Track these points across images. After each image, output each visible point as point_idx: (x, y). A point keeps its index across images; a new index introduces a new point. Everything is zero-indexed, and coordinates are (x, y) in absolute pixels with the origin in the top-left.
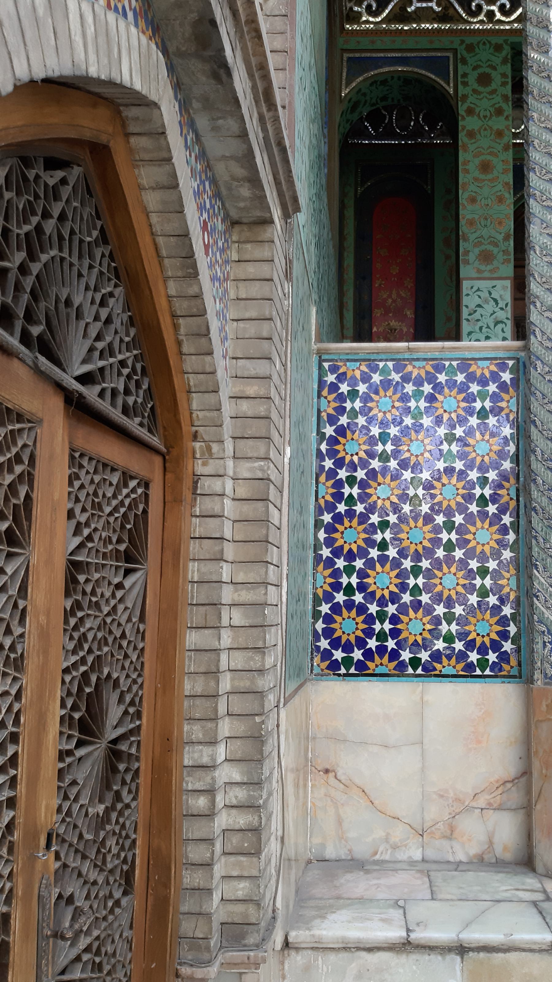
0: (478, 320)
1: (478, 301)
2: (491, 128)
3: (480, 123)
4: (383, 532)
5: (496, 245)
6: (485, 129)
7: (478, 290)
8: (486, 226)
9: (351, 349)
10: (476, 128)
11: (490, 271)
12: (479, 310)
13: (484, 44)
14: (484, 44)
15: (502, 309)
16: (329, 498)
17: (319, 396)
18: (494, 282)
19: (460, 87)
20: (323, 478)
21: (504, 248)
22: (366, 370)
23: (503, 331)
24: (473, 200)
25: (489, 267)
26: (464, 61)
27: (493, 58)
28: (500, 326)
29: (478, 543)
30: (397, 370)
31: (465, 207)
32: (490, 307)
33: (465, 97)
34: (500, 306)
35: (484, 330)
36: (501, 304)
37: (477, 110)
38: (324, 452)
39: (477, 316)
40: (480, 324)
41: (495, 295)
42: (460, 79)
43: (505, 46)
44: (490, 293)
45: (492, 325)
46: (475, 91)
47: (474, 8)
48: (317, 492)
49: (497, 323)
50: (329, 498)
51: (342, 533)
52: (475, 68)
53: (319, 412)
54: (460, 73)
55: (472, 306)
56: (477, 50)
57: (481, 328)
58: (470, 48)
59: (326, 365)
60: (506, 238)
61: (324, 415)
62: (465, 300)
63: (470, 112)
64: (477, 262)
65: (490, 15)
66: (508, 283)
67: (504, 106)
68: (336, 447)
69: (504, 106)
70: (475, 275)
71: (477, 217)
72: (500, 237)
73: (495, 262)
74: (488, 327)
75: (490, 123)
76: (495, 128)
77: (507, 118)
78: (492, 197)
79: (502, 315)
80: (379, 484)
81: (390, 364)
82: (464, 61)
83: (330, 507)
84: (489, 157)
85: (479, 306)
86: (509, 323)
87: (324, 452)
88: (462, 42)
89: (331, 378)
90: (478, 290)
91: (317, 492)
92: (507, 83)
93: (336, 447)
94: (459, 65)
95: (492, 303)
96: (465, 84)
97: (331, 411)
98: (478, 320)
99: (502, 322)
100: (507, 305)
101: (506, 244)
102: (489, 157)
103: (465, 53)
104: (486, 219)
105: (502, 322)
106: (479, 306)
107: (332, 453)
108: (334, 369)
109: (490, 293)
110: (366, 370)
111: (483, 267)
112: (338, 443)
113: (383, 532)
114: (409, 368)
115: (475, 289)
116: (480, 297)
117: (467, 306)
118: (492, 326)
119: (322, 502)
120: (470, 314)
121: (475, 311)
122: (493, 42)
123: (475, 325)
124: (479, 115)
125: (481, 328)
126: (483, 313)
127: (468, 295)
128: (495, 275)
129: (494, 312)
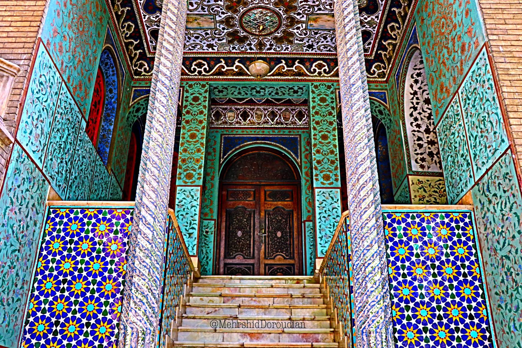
0: (183, 205)
1: (184, 196)
2: (197, 119)
3: (192, 117)
4: (64, 284)
5: (195, 171)
6: (194, 120)
7: (184, 191)
8: (191, 162)
9: (62, 203)
10: (190, 119)
11: (191, 183)
12: (184, 201)
13: (197, 84)
14: (197, 84)
15: (195, 200)
16: (42, 268)
17: (46, 223)
18: (192, 188)
19: (184, 102)
20: (41, 259)
21: (198, 172)
22: (68, 212)
23: (195, 211)
24: (185, 150)
25: (191, 181)
26: (187, 91)
27: (200, 90)
28: (194, 208)
29: (106, 290)
30: (81, 212)
31: (181, 154)
32: (189, 199)
33: (186, 106)
34: (194, 199)
35: (186, 210)
36: (195, 198)
37: (191, 112)
38: (44, 247)
39: (182, 203)
40: (184, 207)
41: (192, 194)
42: (184, 99)
43: (207, 85)
44: (190, 193)
45: (189, 208)
46: (191, 104)
47: (192, 69)
48: (37, 265)
49: (192, 207)
50: (42, 268)
51: (45, 284)
52: (192, 94)
53: (45, 230)
54: (185, 96)
55: (181, 198)
56: (194, 87)
57: (184, 209)
58: (190, 86)
59: (51, 210)
60: (200, 167)
61: (47, 232)
62: (178, 196)
63: (188, 112)
64: (185, 178)
65: (200, 72)
66: (199, 188)
67: (204, 110)
68: (49, 246)
69: (204, 110)
70: (184, 184)
71: (187, 158)
72: (197, 167)
73: (194, 179)
74: (188, 209)
75: (197, 117)
76: (199, 119)
77: (205, 115)
78: (195, 149)
79: (195, 203)
80: (66, 262)
81: (79, 210)
82: (187, 91)
83: (42, 272)
84: (195, 132)
85: (184, 199)
86: (198, 207)
87: (44, 247)
88: (187, 83)
89: (52, 216)
90: (184, 191)
91: (37, 265)
92: (206, 100)
93: (49, 246)
94: (185, 93)
95: (191, 197)
96: (187, 101)
97: (50, 230)
98: (183, 205)
99: (195, 206)
100: (198, 198)
101: (200, 170)
102: (195, 132)
103: (188, 88)
104: (191, 159)
105: (195, 206)
106: (184, 199)
107: (47, 248)
108: (54, 212)
109: (190, 193)
110: (68, 212)
111: (187, 181)
112: (51, 243)
113: (64, 284)
114: (87, 212)
115: (183, 190)
116: (185, 194)
117: (178, 199)
118: (189, 208)
119: (39, 270)
120: (179, 202)
121: (182, 201)
122: (201, 83)
123: (181, 207)
124: (192, 114)
125: (184, 209)
126: (186, 202)
127: (179, 193)
128: (193, 184)
129: (191, 202)
